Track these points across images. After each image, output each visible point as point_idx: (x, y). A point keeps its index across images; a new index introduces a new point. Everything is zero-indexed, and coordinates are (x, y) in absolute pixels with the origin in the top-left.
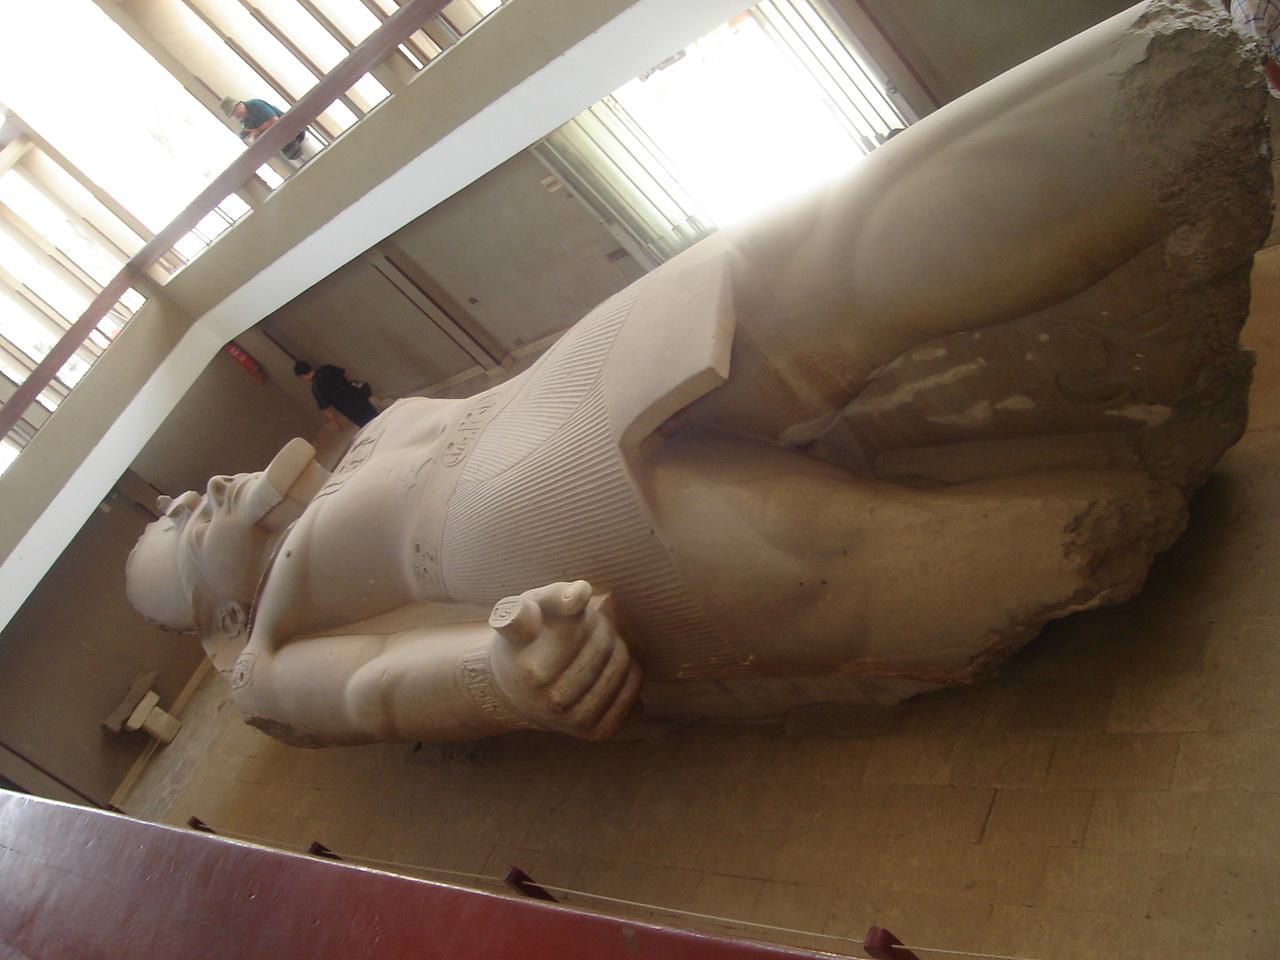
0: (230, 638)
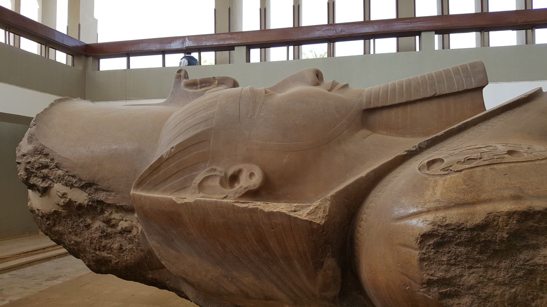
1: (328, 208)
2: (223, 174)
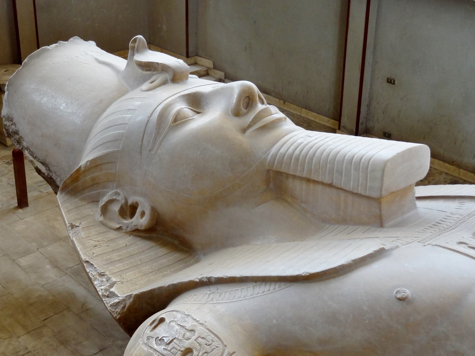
0: (102, 223)
1: (127, 306)
2: (123, 201)
